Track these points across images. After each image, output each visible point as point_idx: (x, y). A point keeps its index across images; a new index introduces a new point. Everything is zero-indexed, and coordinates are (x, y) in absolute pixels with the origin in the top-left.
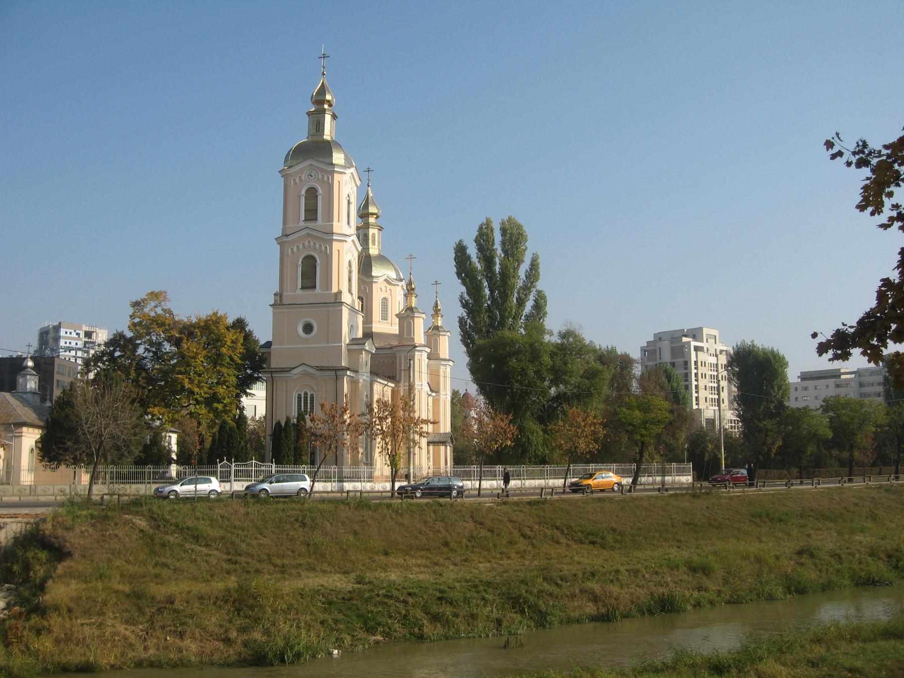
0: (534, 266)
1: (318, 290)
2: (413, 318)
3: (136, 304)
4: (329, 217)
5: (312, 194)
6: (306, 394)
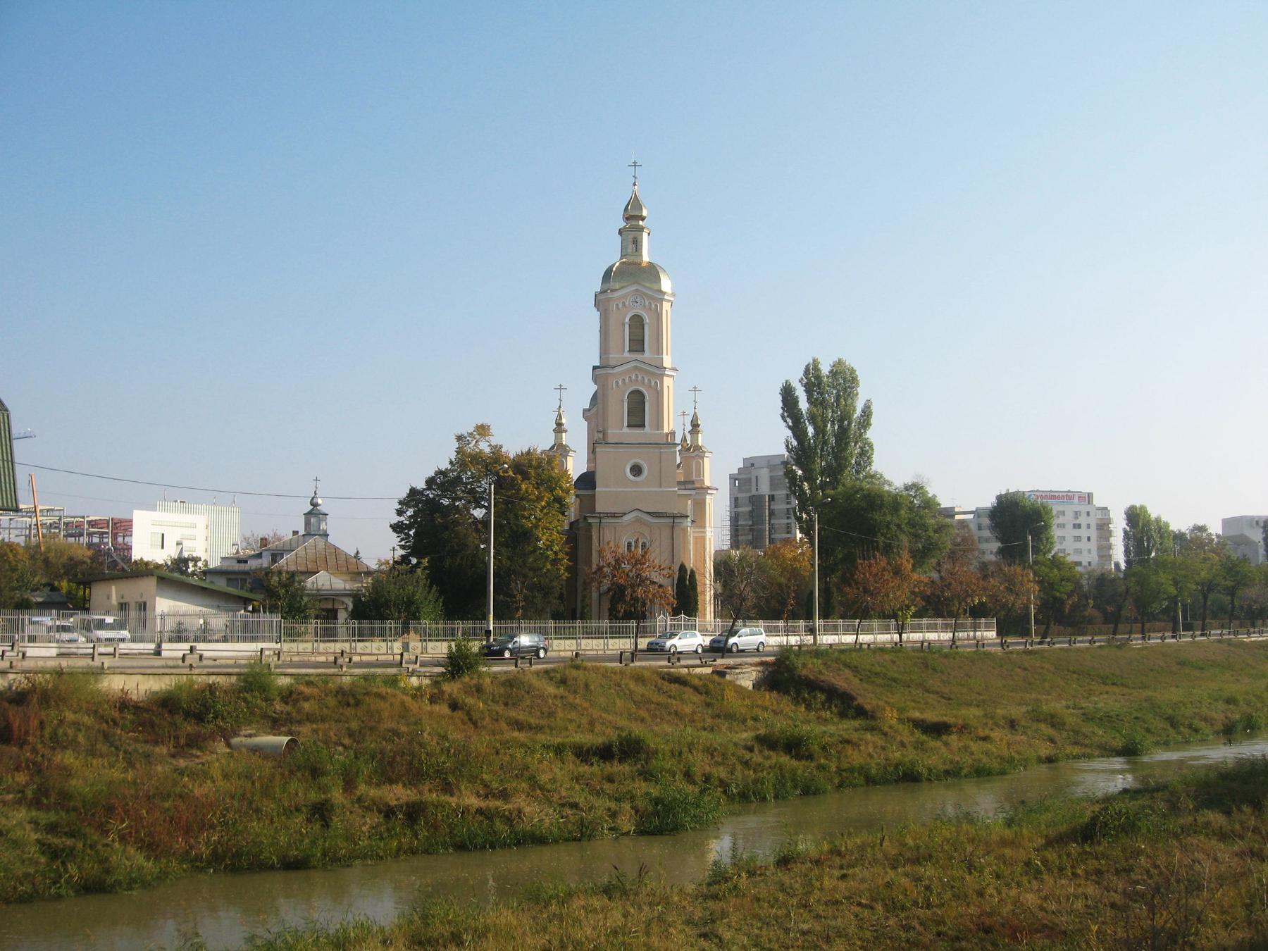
0: (867, 413)
1: (647, 429)
2: (702, 458)
3: (460, 438)
4: (658, 350)
5: (637, 322)
6: (636, 541)
